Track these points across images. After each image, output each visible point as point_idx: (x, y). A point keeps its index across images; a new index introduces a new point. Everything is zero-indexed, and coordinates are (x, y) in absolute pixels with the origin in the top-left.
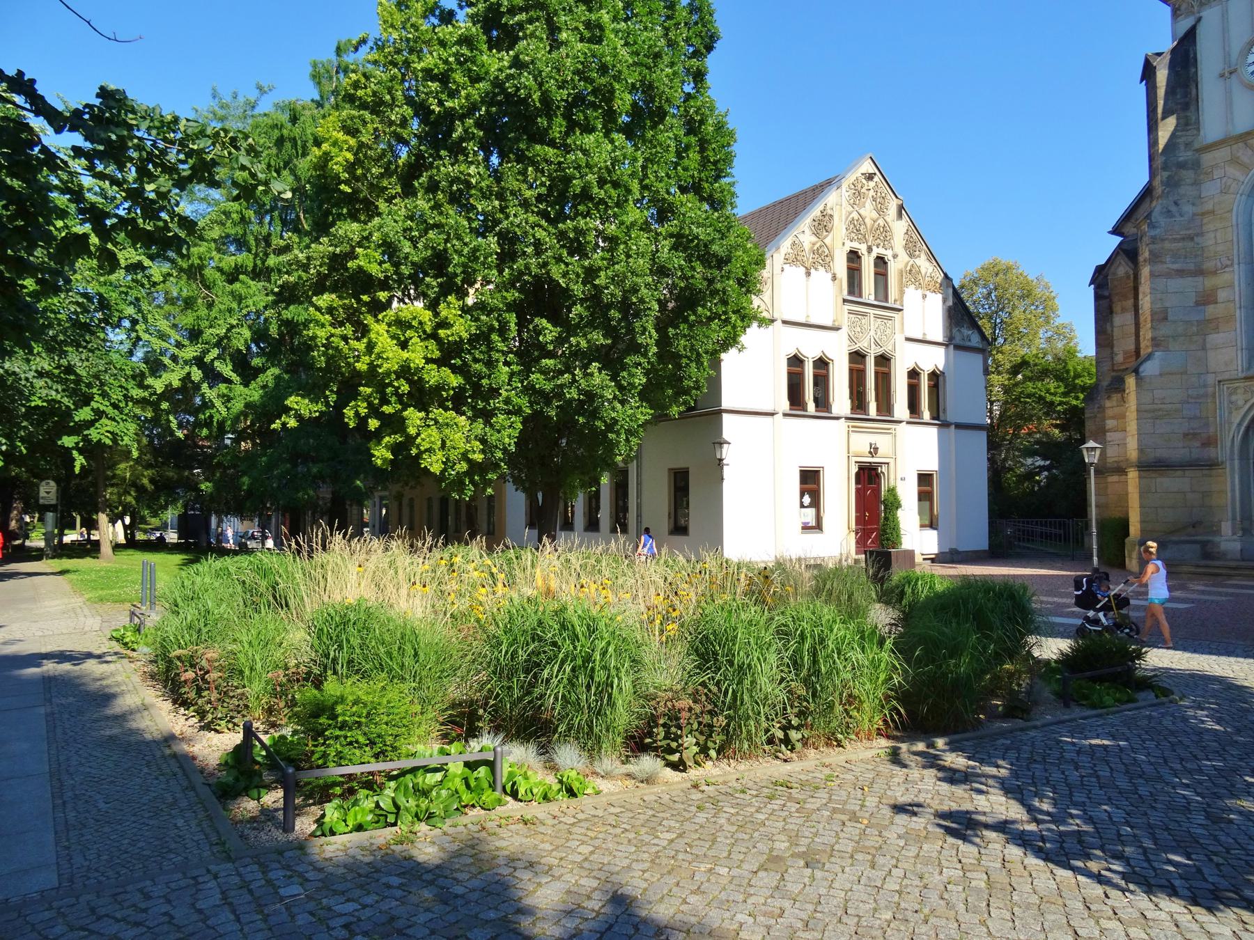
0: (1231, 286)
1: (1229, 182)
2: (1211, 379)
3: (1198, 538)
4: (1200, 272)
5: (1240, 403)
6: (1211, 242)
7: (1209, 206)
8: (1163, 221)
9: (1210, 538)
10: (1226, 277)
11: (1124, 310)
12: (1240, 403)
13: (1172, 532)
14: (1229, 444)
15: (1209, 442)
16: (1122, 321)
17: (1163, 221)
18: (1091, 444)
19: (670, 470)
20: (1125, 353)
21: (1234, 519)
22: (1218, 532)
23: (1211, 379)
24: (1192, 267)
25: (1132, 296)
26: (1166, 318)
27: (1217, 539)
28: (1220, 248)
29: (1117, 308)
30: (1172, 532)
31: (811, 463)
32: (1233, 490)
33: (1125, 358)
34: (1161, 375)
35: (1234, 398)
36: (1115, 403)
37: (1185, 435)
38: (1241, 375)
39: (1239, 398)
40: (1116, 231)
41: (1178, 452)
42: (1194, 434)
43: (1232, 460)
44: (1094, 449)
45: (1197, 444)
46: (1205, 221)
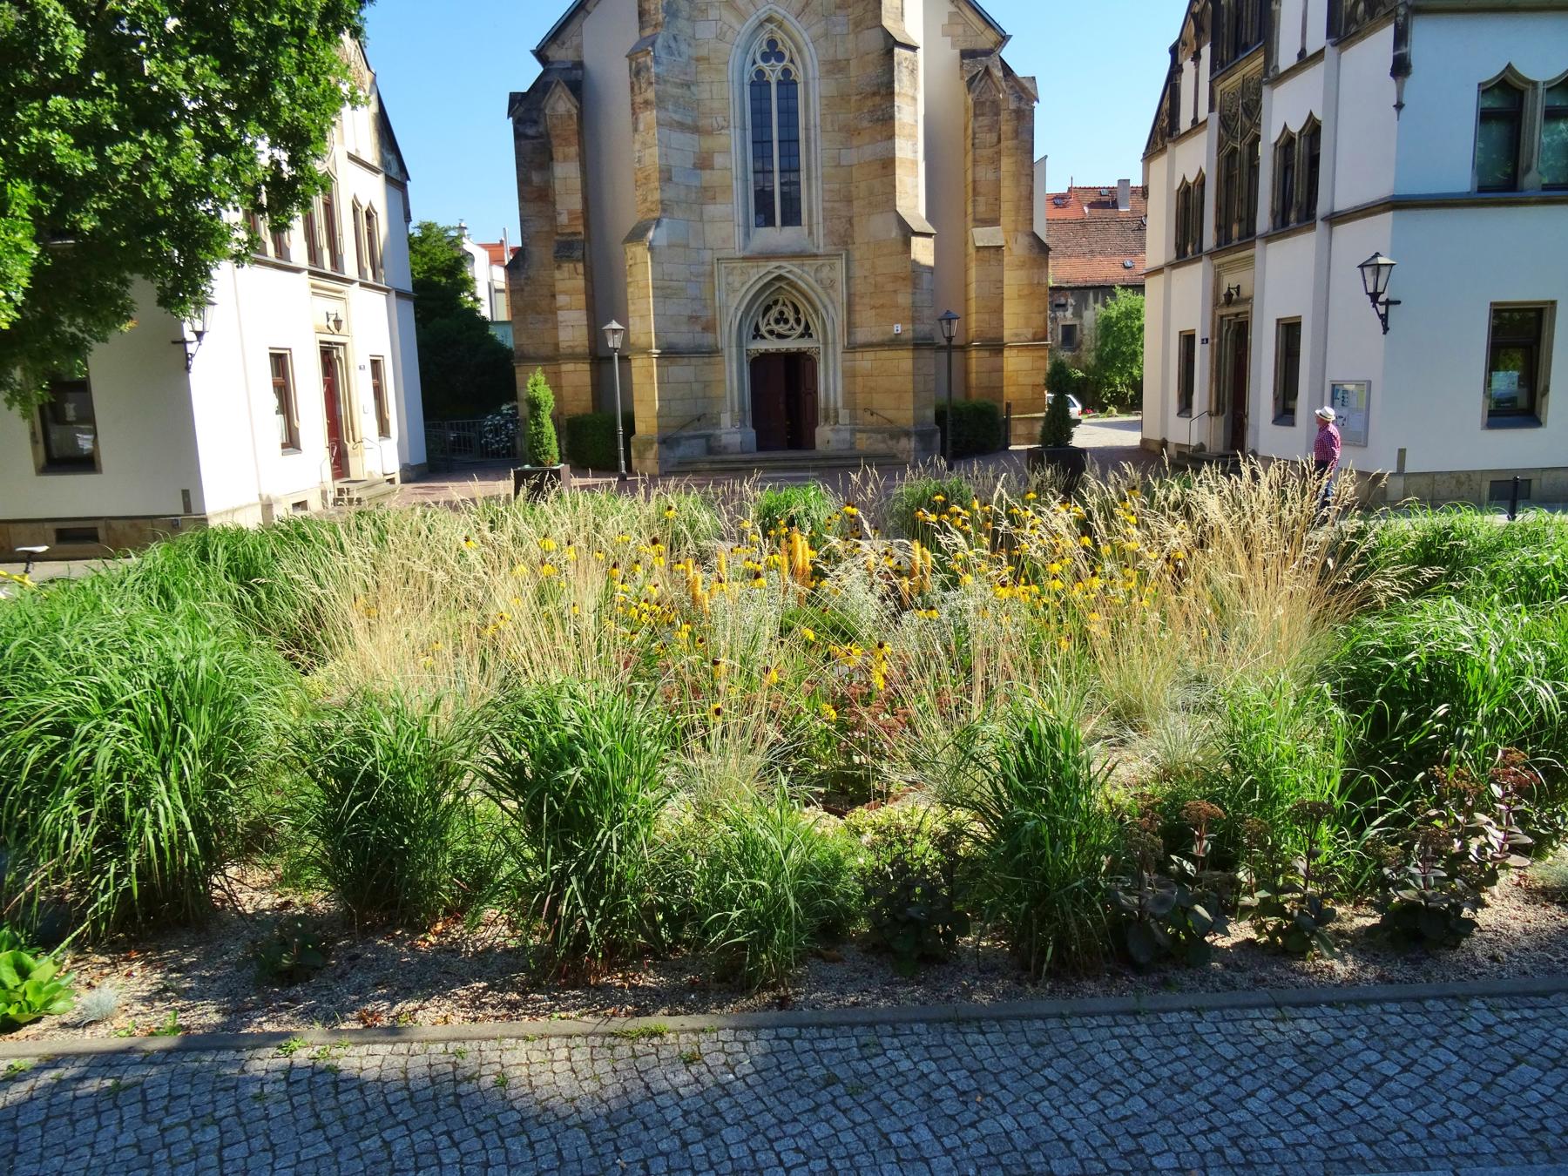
0: (727, 151)
1: (725, 28)
2: (707, 256)
4: (696, 130)
5: (737, 285)
6: (706, 95)
7: (703, 52)
8: (664, 57)
10: (723, 140)
11: (565, 159)
12: (737, 285)
13: (683, 427)
15: (709, 327)
16: (566, 172)
17: (664, 57)
18: (615, 325)
20: (570, 213)
22: (717, 425)
23: (707, 256)
24: (689, 121)
25: (574, 139)
26: (670, 179)
28: (716, 105)
29: (558, 152)
30: (683, 427)
31: (280, 343)
33: (570, 220)
34: (670, 246)
35: (730, 279)
36: (566, 275)
37: (690, 318)
38: (741, 254)
39: (736, 280)
40: (540, 54)
41: (682, 337)
42: (697, 318)
44: (615, 331)
45: (698, 328)
46: (701, 67)
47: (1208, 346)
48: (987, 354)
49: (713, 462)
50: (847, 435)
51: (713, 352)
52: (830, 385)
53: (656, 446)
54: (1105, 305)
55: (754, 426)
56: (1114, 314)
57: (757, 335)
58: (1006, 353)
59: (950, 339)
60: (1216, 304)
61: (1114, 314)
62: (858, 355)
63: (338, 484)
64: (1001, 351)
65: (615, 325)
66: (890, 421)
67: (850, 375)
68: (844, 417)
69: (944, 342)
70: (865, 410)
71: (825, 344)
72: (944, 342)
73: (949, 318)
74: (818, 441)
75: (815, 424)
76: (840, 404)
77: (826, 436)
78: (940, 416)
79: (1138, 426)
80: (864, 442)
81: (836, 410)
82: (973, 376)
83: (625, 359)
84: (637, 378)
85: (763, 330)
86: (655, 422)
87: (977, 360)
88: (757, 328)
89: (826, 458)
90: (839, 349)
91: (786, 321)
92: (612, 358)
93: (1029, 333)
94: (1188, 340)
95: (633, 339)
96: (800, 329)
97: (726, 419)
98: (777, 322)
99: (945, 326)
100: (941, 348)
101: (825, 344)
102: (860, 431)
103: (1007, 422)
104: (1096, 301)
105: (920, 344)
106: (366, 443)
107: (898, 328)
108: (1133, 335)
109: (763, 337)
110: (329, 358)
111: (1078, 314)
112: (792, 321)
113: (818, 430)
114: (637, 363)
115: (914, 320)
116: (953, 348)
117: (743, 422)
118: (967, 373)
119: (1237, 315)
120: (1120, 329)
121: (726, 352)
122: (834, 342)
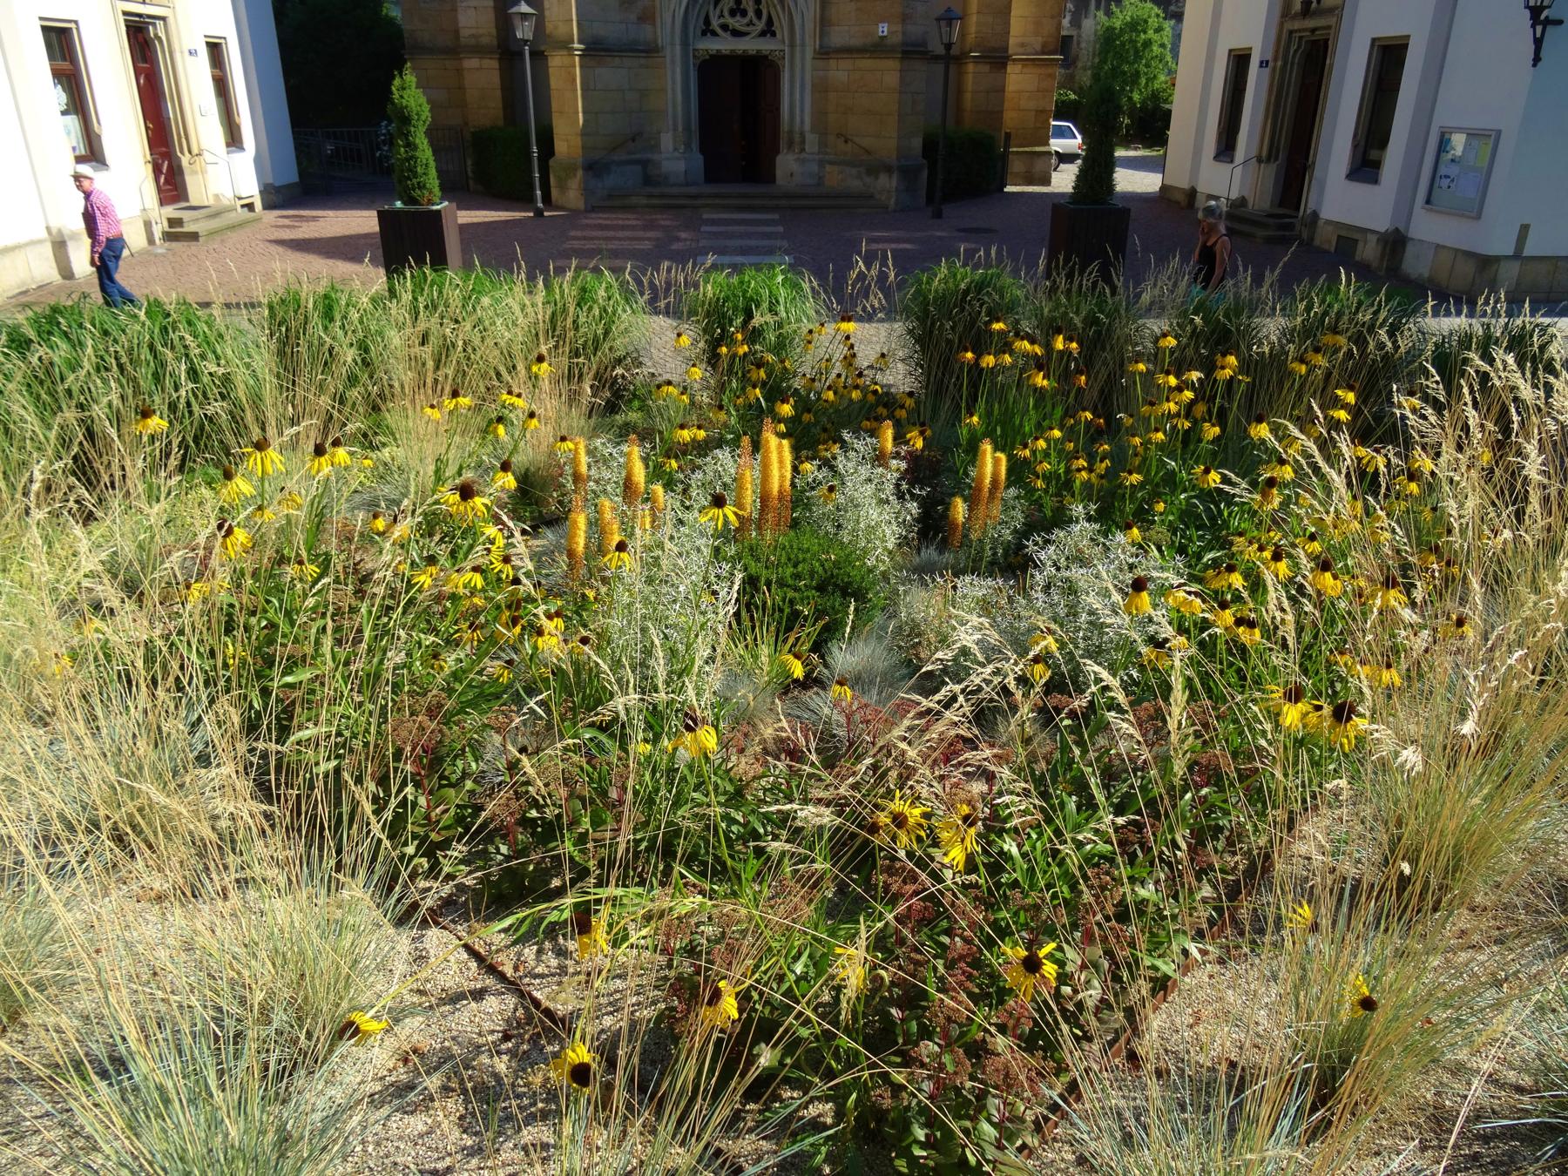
3: (638, 156)
9: (649, 156)
14: (669, 20)
18: (524, 8)
19: (1374, 40)
21: (675, 129)
22: (656, 147)
27: (656, 157)
31: (60, 11)
32: (674, 90)
43: (673, 44)
44: (525, 16)
45: (633, 17)
47: (1267, 71)
48: (986, 68)
49: (650, 196)
50: (815, 168)
51: (651, 50)
52: (796, 102)
53: (580, 173)
54: (1109, 13)
55: (702, 151)
56: (1118, 24)
57: (707, 31)
58: (1009, 69)
59: (948, 46)
60: (1286, 14)
61: (1118, 24)
62: (833, 63)
63: (170, 211)
64: (1004, 66)
65: (524, 8)
66: (868, 152)
67: (822, 88)
68: (811, 139)
69: (941, 51)
70: (839, 135)
71: (792, 46)
72: (941, 51)
73: (948, 18)
74: (779, 173)
75: (776, 151)
76: (807, 126)
77: (788, 167)
78: (929, 147)
79: (1158, 165)
80: (835, 178)
81: (802, 134)
82: (968, 96)
83: (539, 56)
84: (555, 82)
85: (715, 23)
86: (577, 142)
87: (973, 76)
88: (707, 21)
89: (788, 196)
90: (809, 54)
91: (744, 13)
92: (521, 54)
93: (1037, 43)
94: (1240, 61)
95: (549, 27)
96: (761, 25)
97: (667, 141)
98: (733, 13)
99: (945, 29)
100: (937, 58)
101: (792, 46)
102: (831, 163)
103: (1004, 157)
104: (1098, 8)
105: (911, 51)
106: (206, 155)
107: (883, 29)
108: (1137, 51)
109: (714, 34)
110: (142, 38)
111: (1076, 23)
112: (751, 14)
113: (780, 159)
114: (556, 61)
115: (905, 18)
116: (952, 59)
117: (688, 145)
118: (960, 91)
119: (1313, 30)
120: (1123, 44)
121: (668, 53)
122: (803, 45)
